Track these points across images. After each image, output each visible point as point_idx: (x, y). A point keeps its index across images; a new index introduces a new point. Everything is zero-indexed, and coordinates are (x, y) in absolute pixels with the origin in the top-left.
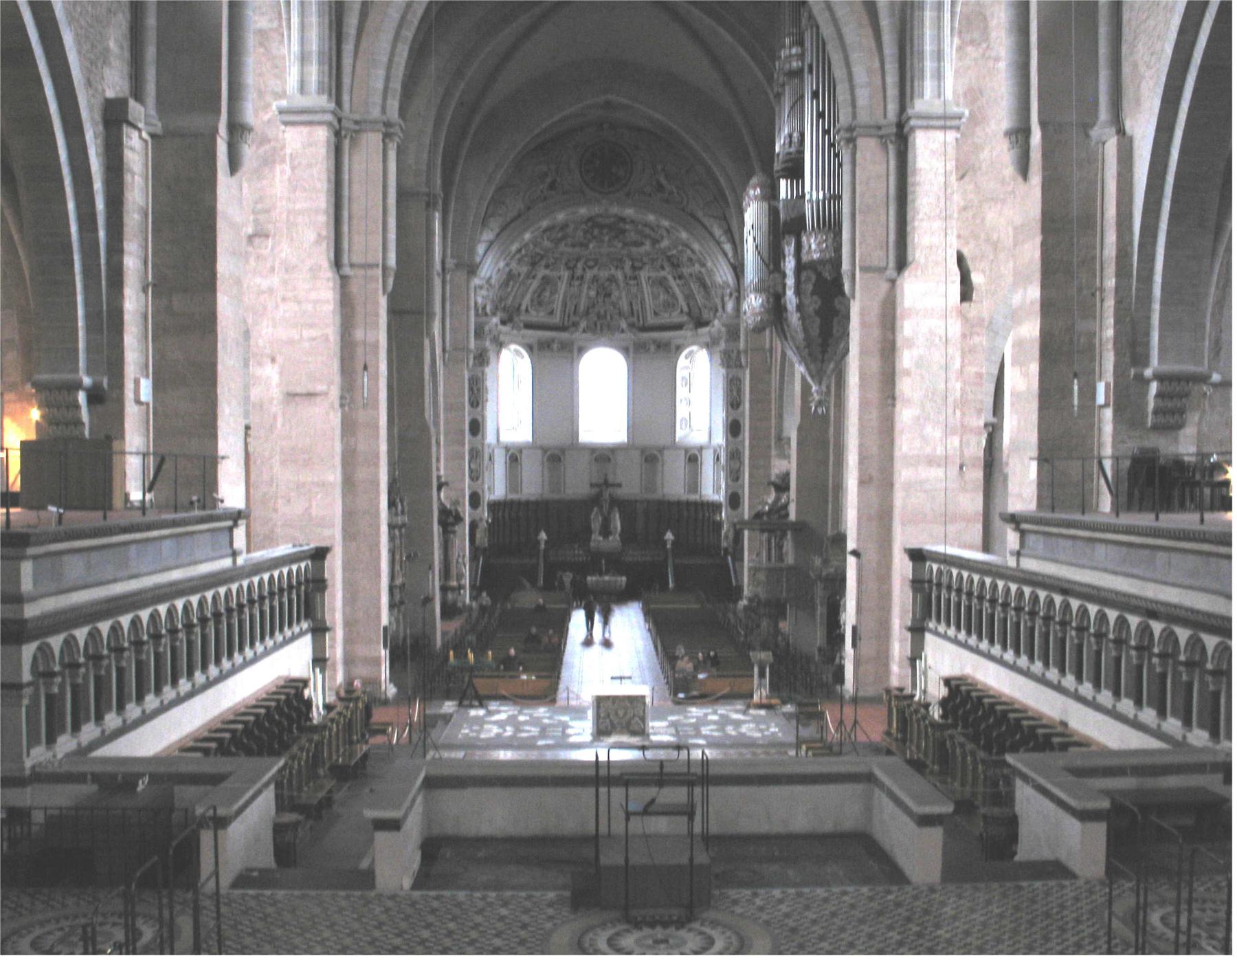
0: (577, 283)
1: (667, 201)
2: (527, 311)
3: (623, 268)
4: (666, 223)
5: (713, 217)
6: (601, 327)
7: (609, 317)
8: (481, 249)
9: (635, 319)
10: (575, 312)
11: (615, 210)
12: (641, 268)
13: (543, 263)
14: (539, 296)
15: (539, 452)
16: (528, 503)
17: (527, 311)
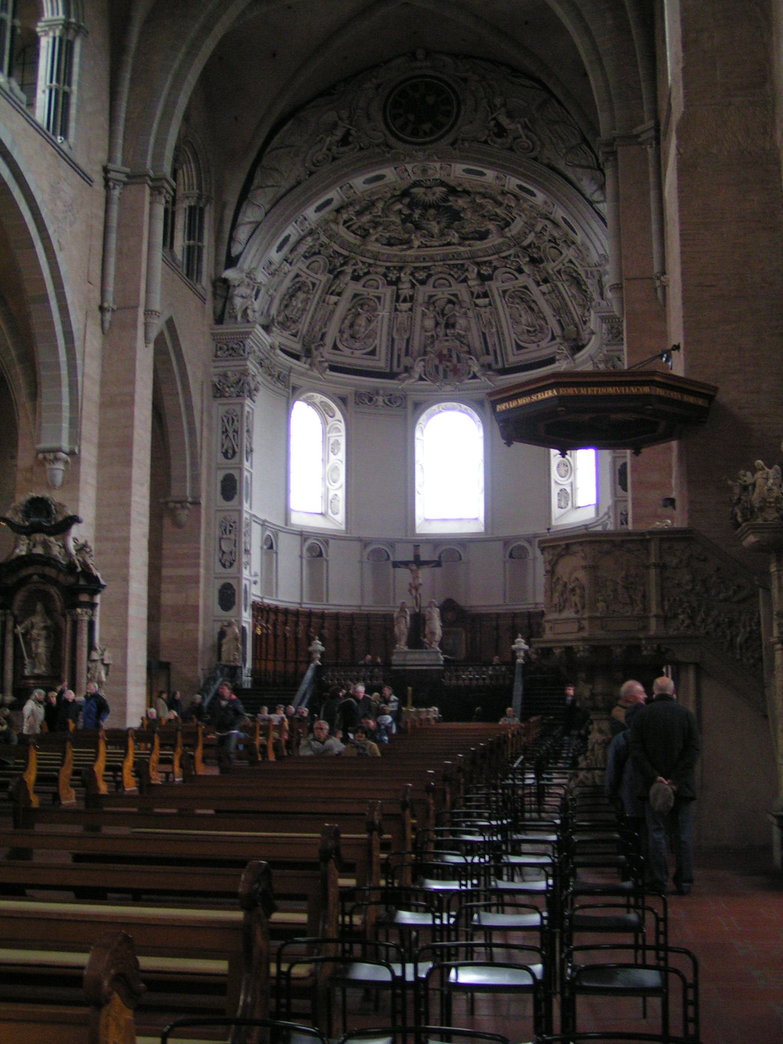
0: (405, 306)
1: (511, 149)
2: (335, 347)
3: (465, 280)
4: (512, 182)
5: (582, 167)
6: (445, 371)
7: (455, 360)
8: (242, 234)
9: (490, 359)
10: (407, 354)
11: (436, 170)
12: (490, 278)
13: (349, 269)
14: (352, 326)
15: (358, 545)
16: (337, 616)
17: (335, 347)
